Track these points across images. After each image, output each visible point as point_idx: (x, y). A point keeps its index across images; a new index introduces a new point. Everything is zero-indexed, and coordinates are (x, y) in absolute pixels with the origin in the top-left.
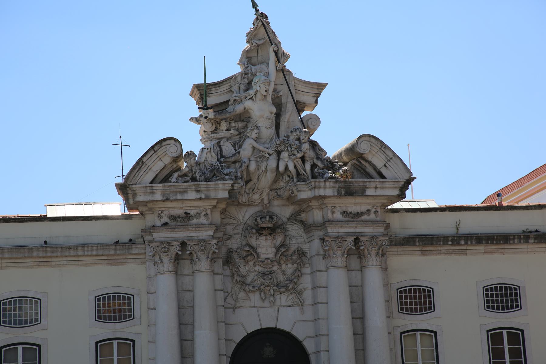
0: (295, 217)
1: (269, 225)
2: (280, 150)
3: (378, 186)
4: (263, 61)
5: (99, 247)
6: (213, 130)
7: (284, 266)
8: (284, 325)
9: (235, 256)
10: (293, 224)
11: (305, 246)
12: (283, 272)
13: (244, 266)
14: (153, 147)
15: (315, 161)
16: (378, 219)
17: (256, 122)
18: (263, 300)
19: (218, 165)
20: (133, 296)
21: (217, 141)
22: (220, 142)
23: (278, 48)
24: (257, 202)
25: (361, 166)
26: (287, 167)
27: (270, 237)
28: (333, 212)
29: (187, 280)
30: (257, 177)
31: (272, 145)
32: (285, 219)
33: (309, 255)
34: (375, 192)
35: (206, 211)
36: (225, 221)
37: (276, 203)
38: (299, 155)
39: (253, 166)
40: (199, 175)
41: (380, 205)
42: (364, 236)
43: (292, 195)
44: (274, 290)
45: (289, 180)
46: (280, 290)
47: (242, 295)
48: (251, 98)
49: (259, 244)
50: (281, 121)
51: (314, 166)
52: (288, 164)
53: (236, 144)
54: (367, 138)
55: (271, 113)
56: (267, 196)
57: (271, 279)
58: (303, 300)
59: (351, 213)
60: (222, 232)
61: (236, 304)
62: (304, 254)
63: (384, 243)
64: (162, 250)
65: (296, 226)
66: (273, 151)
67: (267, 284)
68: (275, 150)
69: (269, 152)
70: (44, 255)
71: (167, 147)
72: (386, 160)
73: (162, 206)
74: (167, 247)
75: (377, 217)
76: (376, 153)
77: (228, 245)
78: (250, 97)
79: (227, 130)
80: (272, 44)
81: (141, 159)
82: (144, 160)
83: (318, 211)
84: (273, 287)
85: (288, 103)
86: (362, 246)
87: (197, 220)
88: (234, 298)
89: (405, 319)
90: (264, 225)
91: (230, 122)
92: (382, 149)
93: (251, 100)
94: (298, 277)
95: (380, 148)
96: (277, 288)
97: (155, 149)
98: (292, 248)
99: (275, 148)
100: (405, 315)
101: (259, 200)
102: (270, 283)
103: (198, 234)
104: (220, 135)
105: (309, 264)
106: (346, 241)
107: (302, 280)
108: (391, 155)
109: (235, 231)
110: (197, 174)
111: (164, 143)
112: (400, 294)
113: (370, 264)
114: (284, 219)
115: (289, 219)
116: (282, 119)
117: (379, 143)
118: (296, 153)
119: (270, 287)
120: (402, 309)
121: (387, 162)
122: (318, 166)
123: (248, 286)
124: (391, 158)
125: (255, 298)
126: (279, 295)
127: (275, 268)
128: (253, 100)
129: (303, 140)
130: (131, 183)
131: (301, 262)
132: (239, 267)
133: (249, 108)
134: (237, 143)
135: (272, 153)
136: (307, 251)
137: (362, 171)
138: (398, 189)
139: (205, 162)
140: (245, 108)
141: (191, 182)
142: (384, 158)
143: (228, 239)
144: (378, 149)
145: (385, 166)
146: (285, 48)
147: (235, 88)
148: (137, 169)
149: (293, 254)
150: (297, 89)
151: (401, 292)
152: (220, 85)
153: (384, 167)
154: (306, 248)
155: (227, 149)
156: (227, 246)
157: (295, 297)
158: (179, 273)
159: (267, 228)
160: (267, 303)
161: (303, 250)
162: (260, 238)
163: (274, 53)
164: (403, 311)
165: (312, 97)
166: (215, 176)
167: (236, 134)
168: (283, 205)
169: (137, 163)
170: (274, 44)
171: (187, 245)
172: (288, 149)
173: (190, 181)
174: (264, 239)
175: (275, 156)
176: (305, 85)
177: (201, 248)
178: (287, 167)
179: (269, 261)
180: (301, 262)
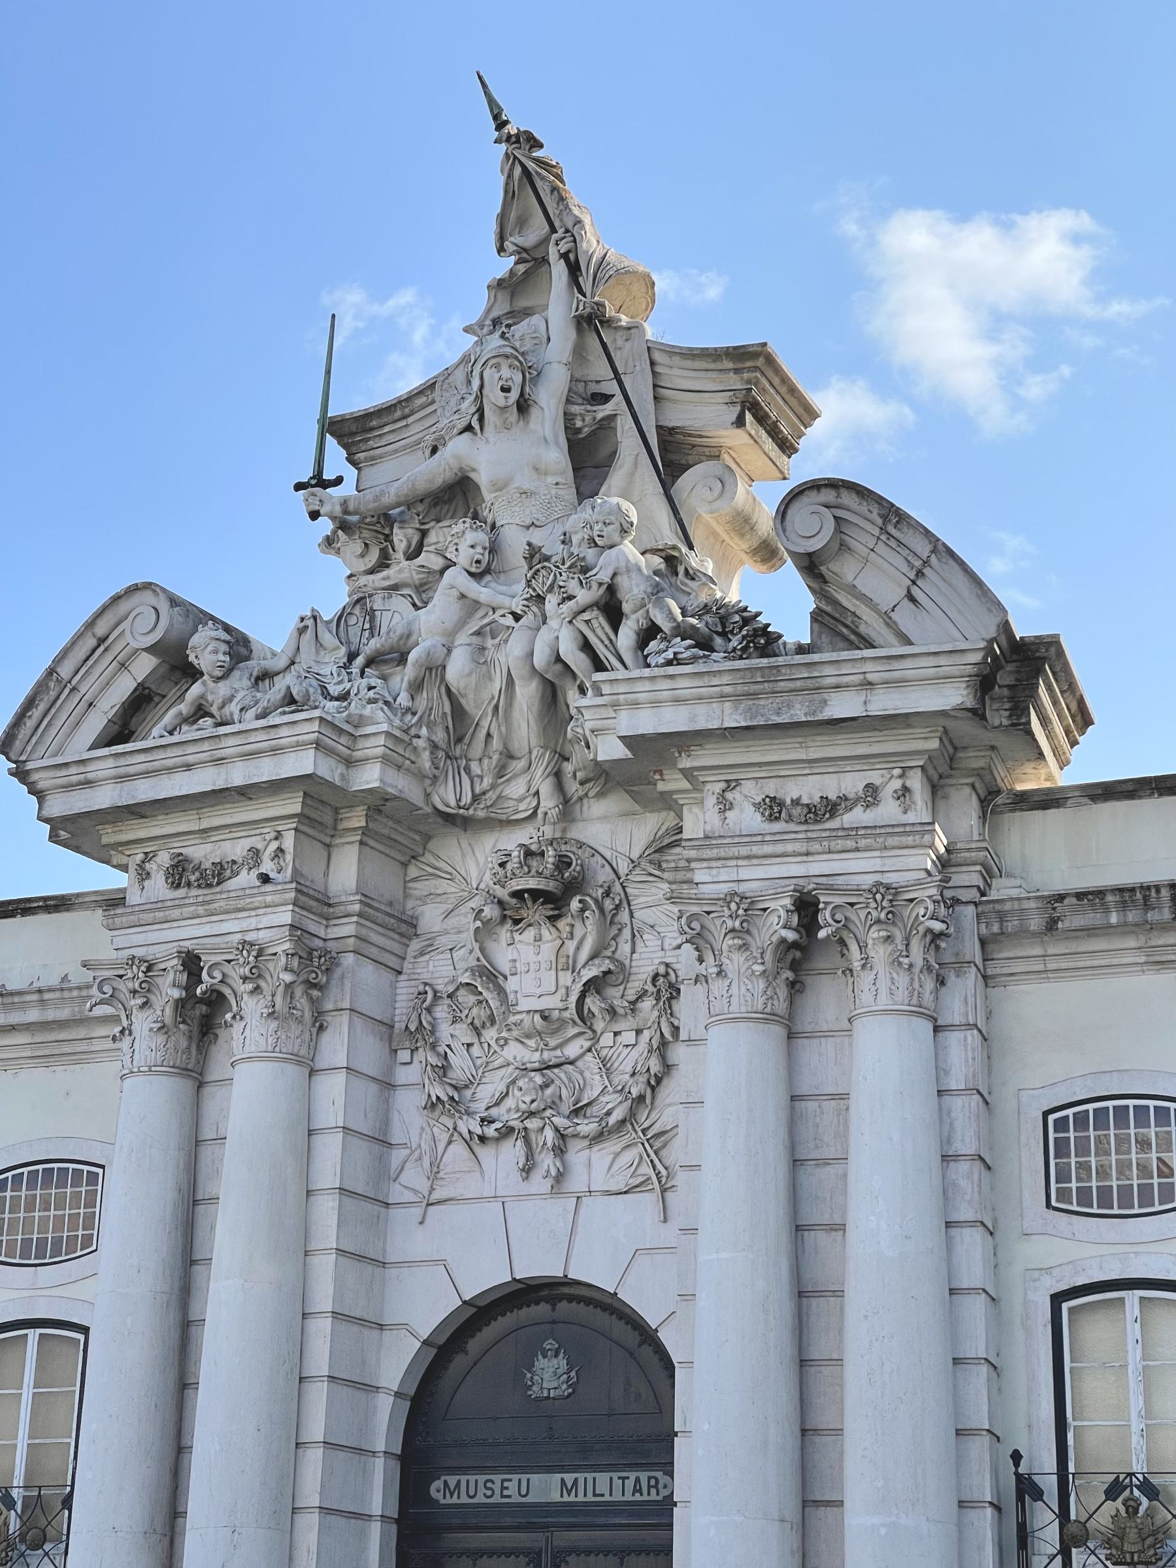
0: (655, 852)
1: (532, 883)
3: (870, 677)
6: (369, 566)
7: (607, 1039)
10: (651, 879)
12: (606, 1066)
16: (911, 818)
20: (103, 1167)
22: (371, 596)
23: (575, 241)
24: (524, 812)
25: (837, 615)
27: (552, 930)
28: (725, 806)
30: (490, 709)
32: (626, 864)
35: (276, 838)
36: (420, 889)
37: (597, 808)
38: (584, 596)
39: (457, 668)
40: (239, 707)
41: (921, 763)
42: (830, 888)
44: (557, 1130)
46: (579, 1128)
48: (469, 428)
49: (515, 961)
56: (550, 781)
57: (546, 1086)
58: (666, 1168)
59: (796, 802)
61: (432, 1190)
63: (922, 912)
69: (514, 609)
72: (912, 576)
73: (142, 834)
74: (141, 974)
75: (905, 812)
76: (872, 550)
77: (419, 974)
78: (463, 424)
84: (553, 1119)
89: (1073, 1238)
91: (422, 527)
92: (891, 529)
93: (467, 435)
95: (881, 529)
96: (566, 1123)
97: (101, 629)
98: (642, 970)
100: (1075, 1218)
101: (528, 800)
102: (533, 1101)
103: (245, 925)
104: (384, 579)
106: (765, 910)
109: (452, 922)
110: (234, 703)
112: (1056, 1131)
113: (866, 998)
115: (634, 864)
117: (876, 505)
118: (573, 586)
119: (543, 1119)
120: (1063, 1195)
121: (914, 583)
123: (465, 1117)
124: (926, 563)
128: (475, 434)
129: (599, 536)
131: (663, 1019)
132: (448, 1051)
135: (524, 608)
137: (852, 637)
138: (964, 685)
142: (904, 568)
143: (422, 954)
144: (876, 532)
145: (912, 599)
150: (662, 384)
151: (1061, 1125)
153: (906, 603)
156: (416, 977)
157: (641, 1157)
160: (539, 1183)
163: (562, 261)
165: (726, 407)
168: (626, 814)
170: (561, 231)
176: (689, 363)
179: (537, 1017)
180: (663, 1019)
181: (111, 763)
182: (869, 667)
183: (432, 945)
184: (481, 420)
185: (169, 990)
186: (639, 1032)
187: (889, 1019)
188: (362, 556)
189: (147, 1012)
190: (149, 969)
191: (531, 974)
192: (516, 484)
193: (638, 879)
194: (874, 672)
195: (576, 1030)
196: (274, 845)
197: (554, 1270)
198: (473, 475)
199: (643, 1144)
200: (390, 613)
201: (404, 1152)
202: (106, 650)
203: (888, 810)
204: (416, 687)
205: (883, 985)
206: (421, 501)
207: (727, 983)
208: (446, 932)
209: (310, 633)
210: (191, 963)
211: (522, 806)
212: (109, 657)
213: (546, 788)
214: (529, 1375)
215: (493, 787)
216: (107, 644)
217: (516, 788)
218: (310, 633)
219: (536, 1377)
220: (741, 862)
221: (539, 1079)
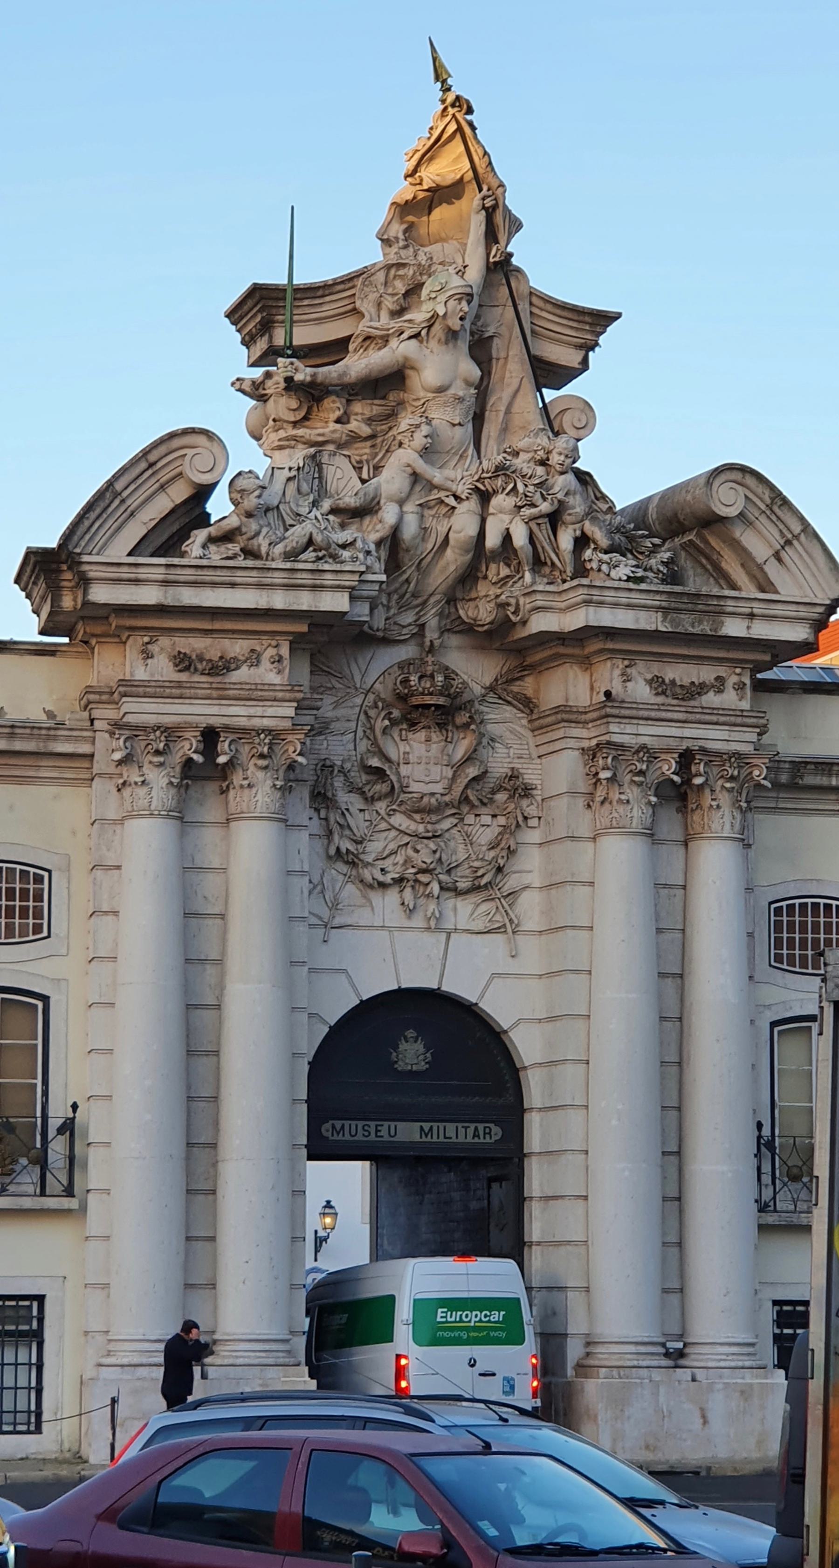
2: (490, 490)
4: (443, 235)
7: (470, 819)
10: (500, 701)
11: (531, 766)
13: (361, 810)
14: (145, 453)
15: (588, 527)
17: (424, 404)
18: (410, 912)
19: (316, 518)
21: (312, 450)
26: (507, 538)
27: (438, 733)
29: (210, 836)
31: (465, 473)
33: (539, 792)
34: (748, 628)
35: (276, 647)
40: (267, 542)
43: (513, 618)
44: (440, 883)
45: (508, 577)
47: (351, 891)
48: (416, 336)
49: (408, 753)
50: (488, 407)
51: (582, 541)
52: (511, 531)
53: (365, 462)
54: (737, 476)
57: (435, 852)
62: (527, 791)
64: (150, 747)
65: (509, 708)
66: (470, 491)
68: (476, 487)
69: (458, 493)
71: (185, 455)
75: (740, 700)
79: (338, 421)
80: (480, 190)
81: (110, 484)
84: (440, 876)
85: (509, 358)
86: (698, 775)
87: (252, 668)
88: (327, 897)
93: (413, 342)
94: (511, 852)
97: (152, 458)
98: (495, 770)
99: (477, 481)
102: (432, 863)
103: (252, 711)
104: (319, 435)
105: (540, 818)
110: (261, 537)
114: (478, 690)
115: (491, 688)
116: (491, 403)
118: (537, 498)
122: (595, 543)
126: (453, 900)
132: (346, 812)
133: (407, 365)
134: (368, 461)
136: (535, 782)
139: (281, 507)
141: (245, 559)
146: (513, 202)
147: (366, 306)
148: (98, 511)
152: (327, 292)
155: (339, 474)
157: (497, 908)
159: (433, 708)
160: (418, 921)
161: (525, 776)
166: (311, 549)
167: (364, 435)
169: (100, 495)
171: (221, 739)
172: (515, 488)
173: (243, 557)
174: (423, 739)
175: (473, 504)
177: (260, 749)
178: (507, 538)
181: (162, 570)
183: (328, 728)
186: (494, 816)
187: (729, 843)
191: (422, 767)
192: (451, 391)
193: (491, 700)
199: (499, 899)
200: (334, 468)
203: (729, 699)
205: (728, 819)
207: (630, 807)
211: (405, 631)
212: (153, 480)
214: (394, 1054)
216: (155, 468)
219: (400, 1056)
220: (641, 722)
221: (432, 846)
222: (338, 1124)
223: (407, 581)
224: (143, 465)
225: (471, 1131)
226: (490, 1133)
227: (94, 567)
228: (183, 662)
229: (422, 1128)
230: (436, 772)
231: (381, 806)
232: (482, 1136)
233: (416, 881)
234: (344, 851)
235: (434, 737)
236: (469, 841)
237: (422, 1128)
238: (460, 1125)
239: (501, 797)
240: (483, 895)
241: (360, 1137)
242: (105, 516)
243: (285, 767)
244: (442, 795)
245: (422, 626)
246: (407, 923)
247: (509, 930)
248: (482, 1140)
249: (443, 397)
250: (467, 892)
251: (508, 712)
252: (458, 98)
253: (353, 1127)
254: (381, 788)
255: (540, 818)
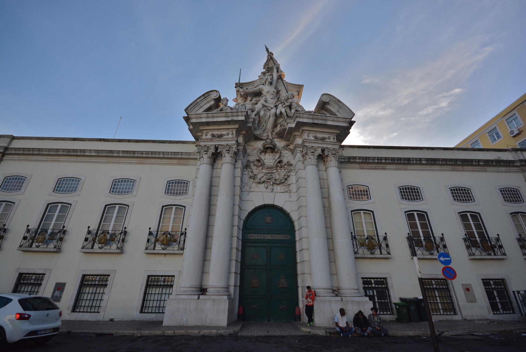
5: (172, 153)
7: (279, 170)
8: (278, 203)
9: (252, 164)
12: (279, 174)
14: (204, 95)
20: (189, 182)
24: (265, 138)
39: (262, 113)
47: (254, 185)
48: (263, 84)
55: (274, 92)
56: (271, 134)
57: (271, 175)
60: (242, 146)
62: (291, 165)
67: (268, 178)
70: (141, 156)
78: (263, 83)
81: (196, 100)
82: (198, 101)
83: (299, 139)
86: (326, 153)
90: (268, 146)
93: (263, 85)
94: (289, 176)
97: (205, 96)
99: (275, 104)
105: (294, 170)
107: (290, 179)
108: (341, 105)
111: (210, 93)
118: (286, 102)
125: (262, 187)
127: (274, 171)
130: (189, 112)
140: (260, 89)
143: (248, 156)
145: (338, 111)
149: (285, 165)
154: (292, 162)
158: (215, 167)
160: (269, 190)
162: (266, 154)
163: (276, 69)
164: (352, 198)
167: (255, 103)
174: (268, 155)
182: (334, 118)
184: (265, 83)
185: (212, 150)
186: (285, 170)
188: (242, 100)
189: (206, 155)
190: (208, 148)
191: (268, 160)
192: (270, 92)
194: (335, 119)
195: (275, 168)
196: (232, 133)
197: (271, 203)
198: (262, 91)
201: (245, 184)
202: (206, 99)
203: (332, 140)
204: (255, 115)
206: (254, 93)
208: (252, 153)
209: (238, 105)
210: (216, 148)
211: (265, 138)
212: (206, 101)
213: (270, 135)
215: (262, 133)
216: (206, 98)
217: (265, 135)
218: (238, 105)
222: (251, 235)
223: (263, 126)
224: (203, 97)
225: (283, 236)
226: (287, 237)
227: (192, 115)
228: (213, 136)
229: (271, 236)
230: (271, 161)
231: (260, 168)
232: (285, 237)
233: (267, 182)
234: (251, 176)
235: (270, 154)
236: (279, 174)
237: (271, 236)
238: (280, 235)
239: (286, 166)
240: (283, 185)
241: (257, 238)
242: (195, 106)
243: (233, 153)
244: (273, 165)
245: (268, 136)
246: (266, 191)
247: (289, 192)
248: (285, 239)
249: (269, 94)
250: (279, 184)
251: (287, 151)
252: (271, 52)
253: (255, 236)
254: (260, 164)
255: (294, 170)
